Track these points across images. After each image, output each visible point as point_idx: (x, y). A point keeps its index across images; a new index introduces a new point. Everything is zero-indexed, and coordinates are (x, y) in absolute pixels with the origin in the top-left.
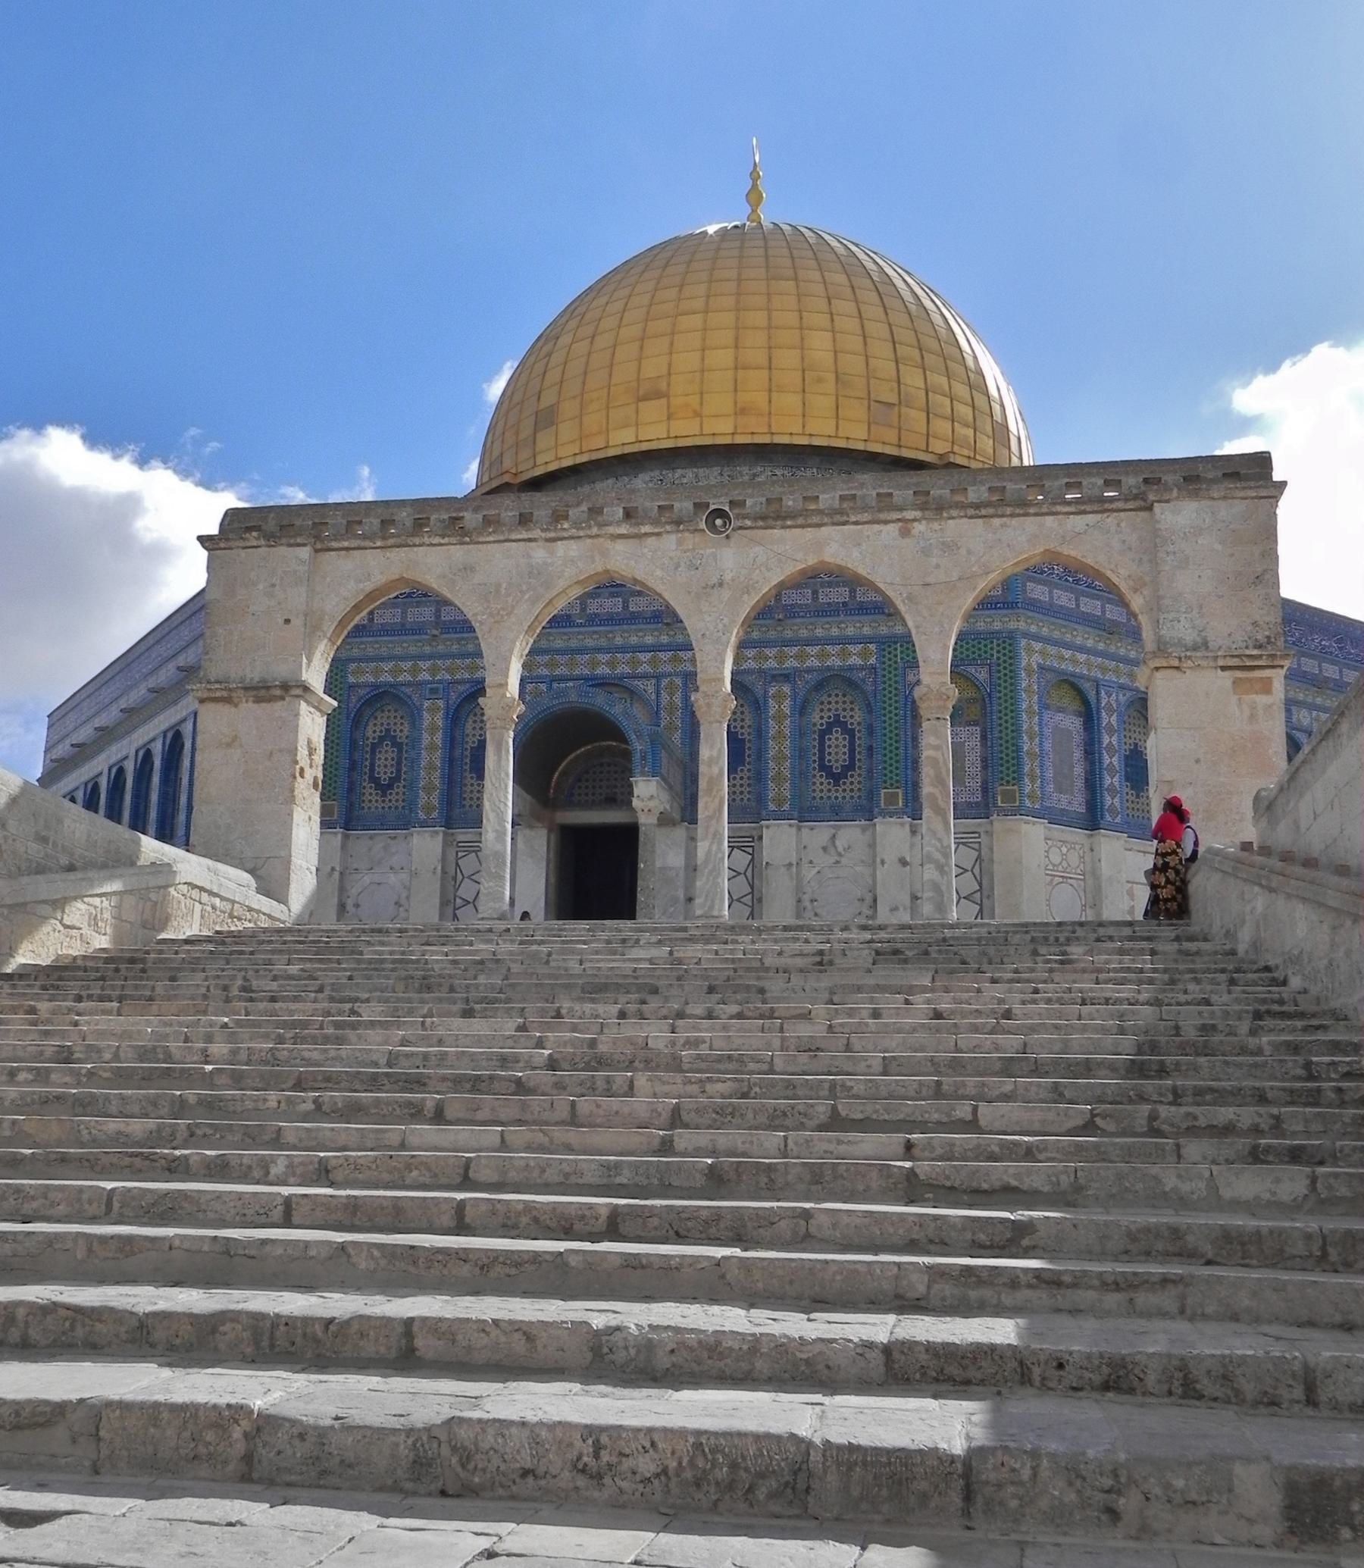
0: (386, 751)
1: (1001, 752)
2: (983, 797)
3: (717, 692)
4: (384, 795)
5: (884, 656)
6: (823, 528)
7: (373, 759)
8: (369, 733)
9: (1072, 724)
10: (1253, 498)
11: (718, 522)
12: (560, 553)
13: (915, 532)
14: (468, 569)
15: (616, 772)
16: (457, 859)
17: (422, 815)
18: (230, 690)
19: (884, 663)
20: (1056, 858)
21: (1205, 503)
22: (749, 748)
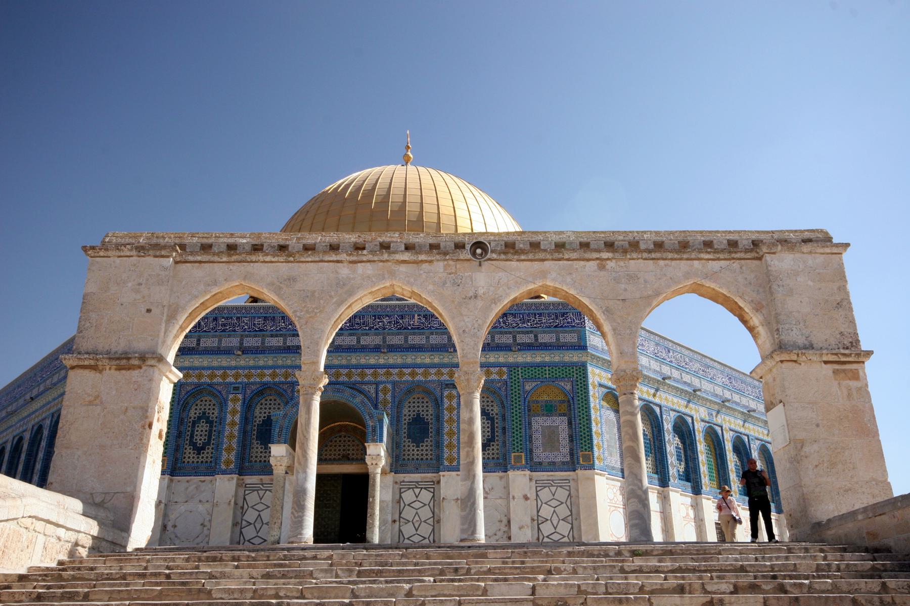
0: (202, 426)
1: (581, 432)
2: (571, 458)
4: (199, 454)
7: (193, 432)
8: (192, 412)
10: (828, 254)
11: (479, 251)
13: (608, 267)
14: (292, 280)
15: (349, 441)
16: (245, 495)
17: (223, 467)
19: (512, 378)
21: (798, 255)
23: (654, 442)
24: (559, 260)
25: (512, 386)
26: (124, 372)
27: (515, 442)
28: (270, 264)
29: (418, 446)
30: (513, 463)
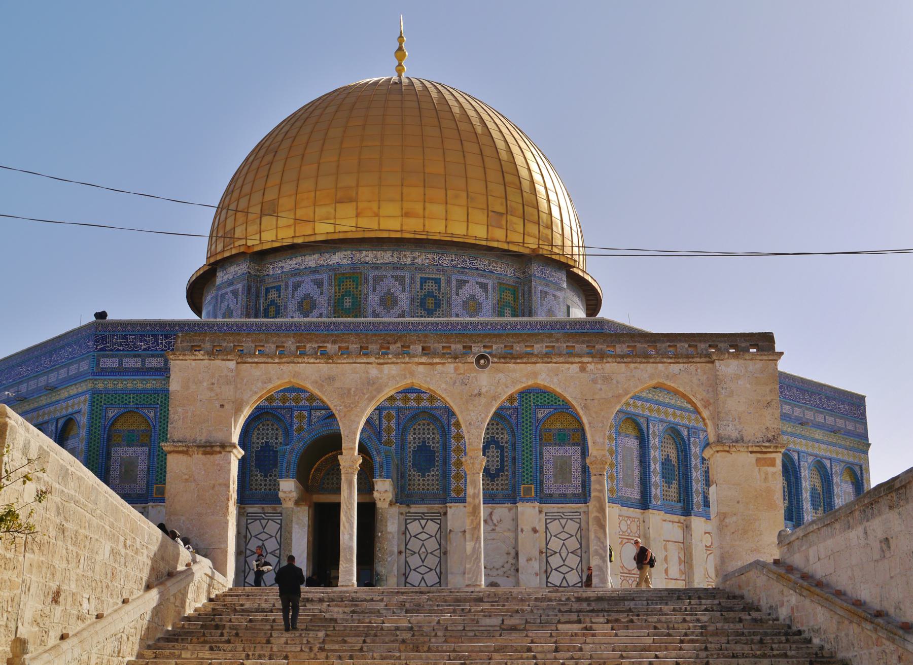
2: (582, 490)
3: (477, 456)
5: (523, 401)
6: (538, 365)
9: (633, 444)
10: (765, 360)
11: (482, 361)
12: (386, 372)
13: (587, 369)
14: (331, 379)
16: (247, 524)
18: (188, 447)
19: (523, 405)
20: (624, 528)
21: (742, 362)
22: (438, 456)
23: (679, 468)
24: (549, 363)
25: (523, 414)
26: (209, 456)
27: (525, 474)
28: (313, 365)
29: (424, 476)
30: (522, 494)
